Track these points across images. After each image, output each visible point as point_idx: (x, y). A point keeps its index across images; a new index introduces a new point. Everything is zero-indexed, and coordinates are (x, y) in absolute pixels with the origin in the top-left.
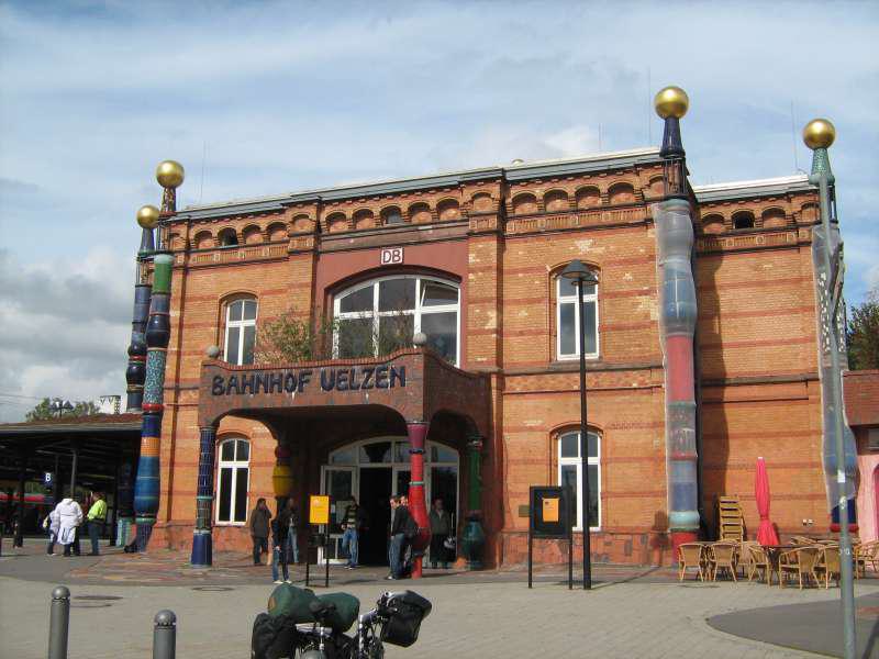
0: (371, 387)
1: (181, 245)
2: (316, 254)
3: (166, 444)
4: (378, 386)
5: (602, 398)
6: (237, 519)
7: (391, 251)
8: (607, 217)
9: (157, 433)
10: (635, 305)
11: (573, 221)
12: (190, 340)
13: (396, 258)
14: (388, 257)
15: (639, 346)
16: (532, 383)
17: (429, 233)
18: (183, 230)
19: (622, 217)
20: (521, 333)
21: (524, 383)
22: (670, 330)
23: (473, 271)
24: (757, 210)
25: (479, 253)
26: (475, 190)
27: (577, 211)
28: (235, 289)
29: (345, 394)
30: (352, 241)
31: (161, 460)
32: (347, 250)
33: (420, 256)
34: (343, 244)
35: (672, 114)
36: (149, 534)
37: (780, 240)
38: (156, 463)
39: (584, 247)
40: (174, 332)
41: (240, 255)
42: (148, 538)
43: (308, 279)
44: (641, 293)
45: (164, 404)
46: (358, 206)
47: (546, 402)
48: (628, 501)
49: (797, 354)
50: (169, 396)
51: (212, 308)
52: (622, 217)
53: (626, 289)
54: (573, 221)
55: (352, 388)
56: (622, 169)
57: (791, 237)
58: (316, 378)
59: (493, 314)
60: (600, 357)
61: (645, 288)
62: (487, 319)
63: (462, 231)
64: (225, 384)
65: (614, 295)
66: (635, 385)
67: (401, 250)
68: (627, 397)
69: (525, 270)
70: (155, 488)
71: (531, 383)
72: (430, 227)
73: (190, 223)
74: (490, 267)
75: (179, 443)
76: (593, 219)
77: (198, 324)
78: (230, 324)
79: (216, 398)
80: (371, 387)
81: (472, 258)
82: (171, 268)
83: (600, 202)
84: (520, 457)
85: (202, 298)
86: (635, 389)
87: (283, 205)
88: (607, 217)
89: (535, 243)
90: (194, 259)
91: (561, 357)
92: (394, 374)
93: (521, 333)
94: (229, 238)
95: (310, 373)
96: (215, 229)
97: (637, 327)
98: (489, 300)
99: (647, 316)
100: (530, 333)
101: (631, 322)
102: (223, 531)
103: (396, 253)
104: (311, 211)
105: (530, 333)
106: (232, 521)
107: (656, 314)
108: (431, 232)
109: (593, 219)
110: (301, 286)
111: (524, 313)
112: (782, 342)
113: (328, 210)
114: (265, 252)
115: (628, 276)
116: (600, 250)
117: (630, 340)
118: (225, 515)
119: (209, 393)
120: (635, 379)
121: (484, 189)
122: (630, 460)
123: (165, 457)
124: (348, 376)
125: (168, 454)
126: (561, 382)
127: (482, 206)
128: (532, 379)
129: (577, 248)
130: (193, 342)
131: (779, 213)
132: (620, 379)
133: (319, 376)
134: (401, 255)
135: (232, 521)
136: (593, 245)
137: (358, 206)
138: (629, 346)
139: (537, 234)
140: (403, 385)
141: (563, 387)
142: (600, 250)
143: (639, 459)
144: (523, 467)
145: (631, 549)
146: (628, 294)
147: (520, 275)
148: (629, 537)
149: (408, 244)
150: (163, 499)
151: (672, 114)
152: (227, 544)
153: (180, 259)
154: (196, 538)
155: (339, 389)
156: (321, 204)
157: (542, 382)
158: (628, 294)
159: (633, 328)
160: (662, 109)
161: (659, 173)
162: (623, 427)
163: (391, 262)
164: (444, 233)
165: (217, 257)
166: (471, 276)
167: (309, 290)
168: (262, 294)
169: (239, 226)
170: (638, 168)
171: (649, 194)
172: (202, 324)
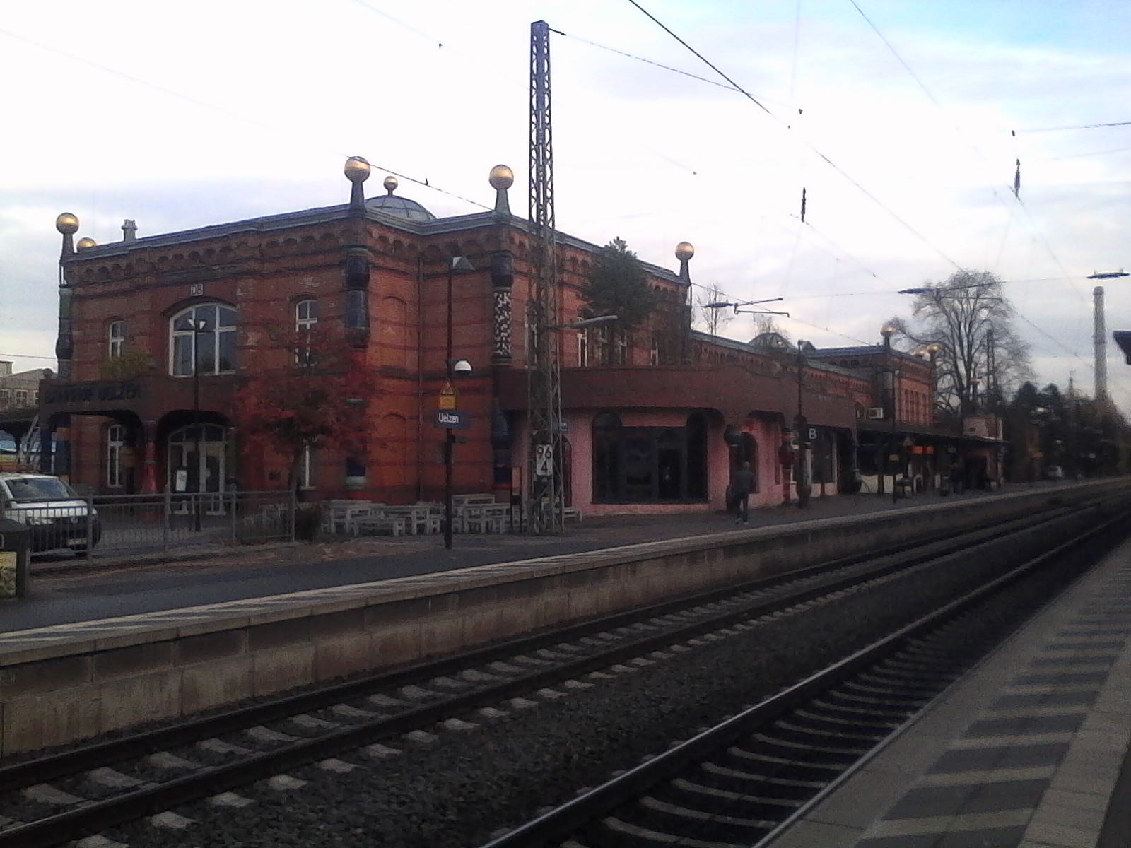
7: (196, 285)
8: (320, 259)
13: (199, 291)
14: (195, 290)
30: (175, 278)
62: (247, 338)
78: (112, 340)
81: (239, 293)
87: (130, 250)
96: (96, 268)
104: (146, 256)
118: (113, 482)
129: (304, 284)
163: (196, 295)
165: (99, 290)
169: (109, 265)
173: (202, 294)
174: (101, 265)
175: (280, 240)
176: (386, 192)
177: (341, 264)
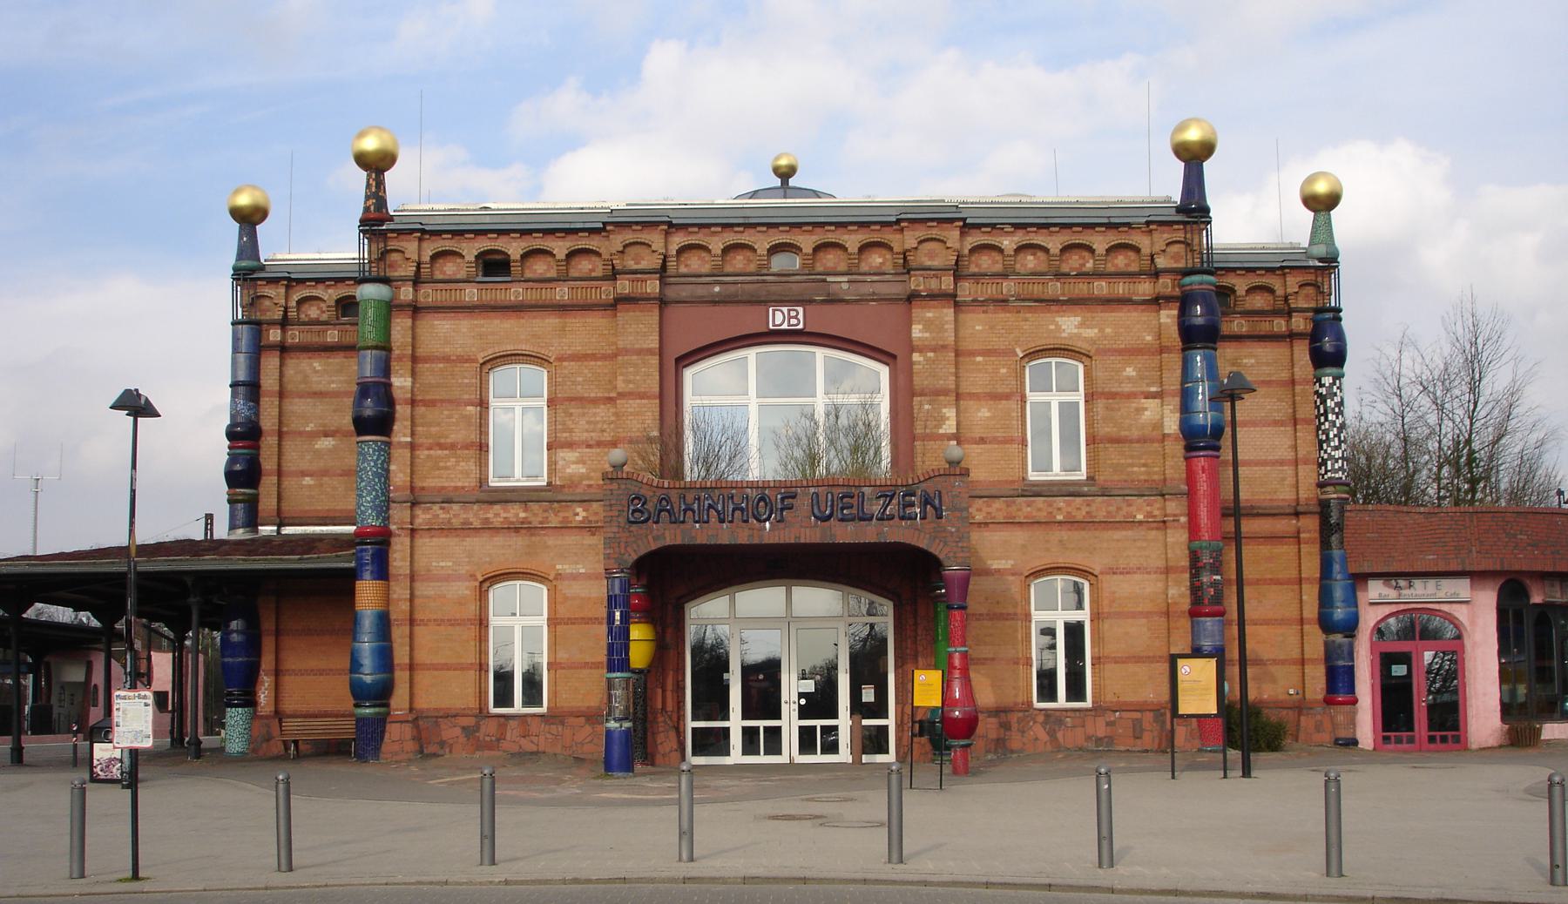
0: (891, 518)
1: (410, 270)
2: (663, 302)
3: (399, 591)
4: (902, 518)
5: (1097, 533)
6: (526, 703)
7: (785, 309)
8: (1101, 287)
9: (382, 572)
10: (1140, 410)
11: (1055, 288)
12: (430, 425)
13: (793, 321)
14: (779, 318)
15: (1144, 465)
16: (999, 510)
17: (841, 284)
18: (411, 247)
19: (1121, 289)
20: (982, 440)
21: (985, 509)
22: (1189, 448)
23: (920, 351)
24: (1240, 284)
25: (928, 325)
26: (921, 232)
27: (1059, 275)
28: (509, 348)
29: (850, 527)
30: (717, 289)
31: (393, 616)
32: (714, 303)
33: (832, 320)
34: (701, 291)
35: (1194, 157)
36: (383, 732)
37: (1264, 327)
38: (384, 623)
39: (1069, 325)
40: (402, 411)
41: (516, 293)
42: (382, 738)
43: (653, 342)
44: (1148, 396)
45: (393, 527)
46: (731, 238)
47: (1019, 536)
48: (1132, 668)
49: (1283, 479)
50: (399, 514)
51: (467, 375)
52: (1121, 289)
53: (1127, 388)
54: (1055, 288)
55: (861, 519)
56: (1128, 225)
57: (1280, 325)
58: (803, 503)
59: (950, 413)
60: (1090, 478)
61: (1153, 389)
62: (943, 419)
63: (895, 289)
64: (650, 506)
65: (1113, 395)
66: (1140, 517)
67: (800, 310)
68: (1130, 533)
69: (987, 353)
70: (385, 657)
71: (998, 508)
72: (845, 279)
73: (425, 233)
74: (944, 347)
75: (423, 589)
76: (1081, 288)
77: (442, 401)
79: (634, 528)
80: (891, 518)
81: (917, 331)
82: (390, 308)
83: (1090, 265)
84: (984, 611)
85: (446, 359)
86: (1140, 522)
88: (1101, 287)
89: (1002, 317)
90: (428, 294)
91: (1033, 476)
92: (927, 501)
93: (982, 440)
94: (493, 265)
95: (794, 497)
96: (471, 249)
97: (1143, 440)
98: (945, 392)
99: (1159, 425)
100: (995, 440)
101: (1135, 433)
102: (512, 723)
103: (793, 314)
104: (656, 239)
105: (995, 440)
106: (518, 707)
107: (1172, 424)
108: (845, 286)
109: (1081, 288)
110: (639, 352)
111: (984, 413)
112: (1264, 463)
113: (678, 240)
114: (562, 293)
115: (1130, 371)
116: (1091, 333)
117: (1132, 457)
119: (622, 520)
120: (1139, 510)
121: (935, 233)
122: (1134, 615)
123: (399, 611)
124: (854, 501)
125: (405, 606)
126: (1039, 510)
127: (931, 255)
128: (998, 504)
129: (1058, 326)
130: (434, 430)
131: (1269, 290)
132: (1119, 509)
133: (807, 502)
134: (801, 316)
135: (518, 707)
136: (1082, 325)
137: (731, 238)
138: (1132, 465)
139: (1002, 302)
140: (940, 517)
141: (1042, 516)
142: (1091, 333)
143: (1147, 615)
144: (987, 623)
145: (1142, 730)
146: (1131, 396)
147: (979, 359)
148: (1137, 715)
149: (811, 302)
150: (401, 677)
151: (1194, 157)
152: (523, 742)
153: (406, 293)
154: (609, 732)
155: (842, 520)
156: (672, 227)
157: (1014, 508)
158: (1131, 396)
159: (1138, 441)
160: (1181, 151)
161: (1180, 236)
162: (1127, 572)
163: (785, 326)
164: (866, 289)
165: (471, 294)
166: (916, 357)
167: (655, 360)
168: (560, 359)
169: (514, 248)
170: (1151, 225)
171: (1161, 262)
172: (450, 401)
173: (801, 326)
174: (484, 244)
175: (1008, 243)
176: (777, 182)
177: (1157, 301)
